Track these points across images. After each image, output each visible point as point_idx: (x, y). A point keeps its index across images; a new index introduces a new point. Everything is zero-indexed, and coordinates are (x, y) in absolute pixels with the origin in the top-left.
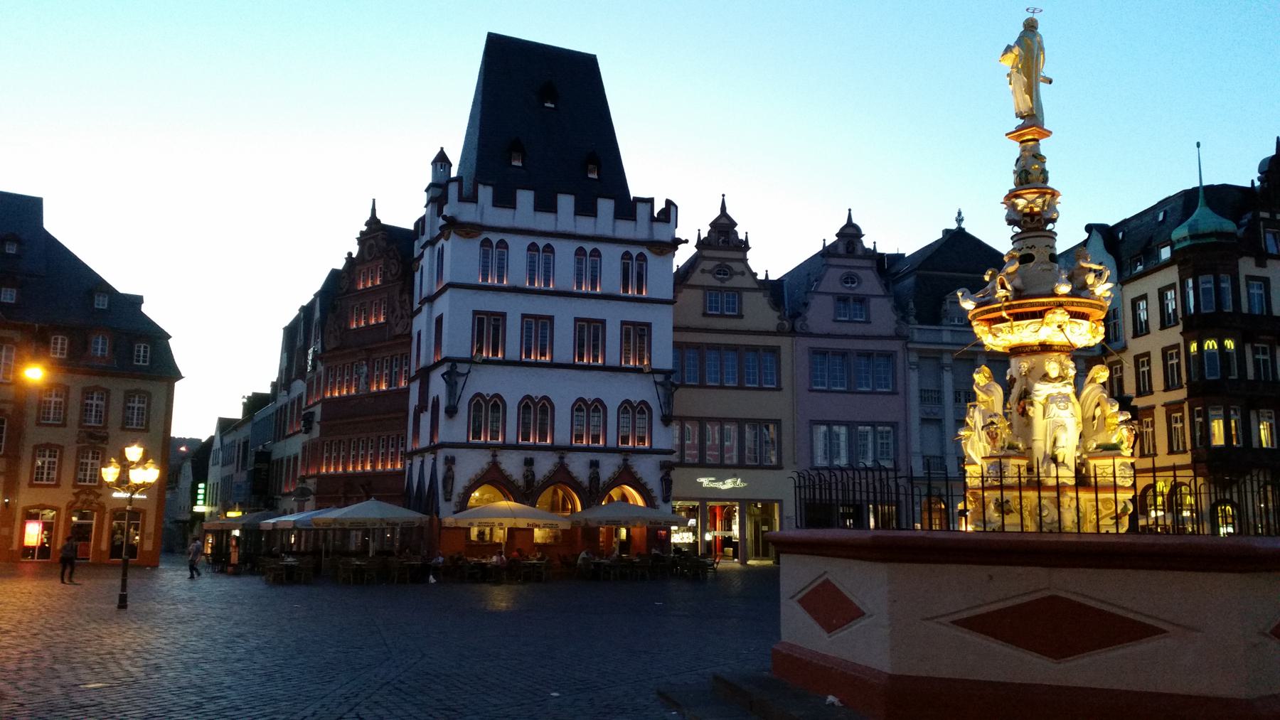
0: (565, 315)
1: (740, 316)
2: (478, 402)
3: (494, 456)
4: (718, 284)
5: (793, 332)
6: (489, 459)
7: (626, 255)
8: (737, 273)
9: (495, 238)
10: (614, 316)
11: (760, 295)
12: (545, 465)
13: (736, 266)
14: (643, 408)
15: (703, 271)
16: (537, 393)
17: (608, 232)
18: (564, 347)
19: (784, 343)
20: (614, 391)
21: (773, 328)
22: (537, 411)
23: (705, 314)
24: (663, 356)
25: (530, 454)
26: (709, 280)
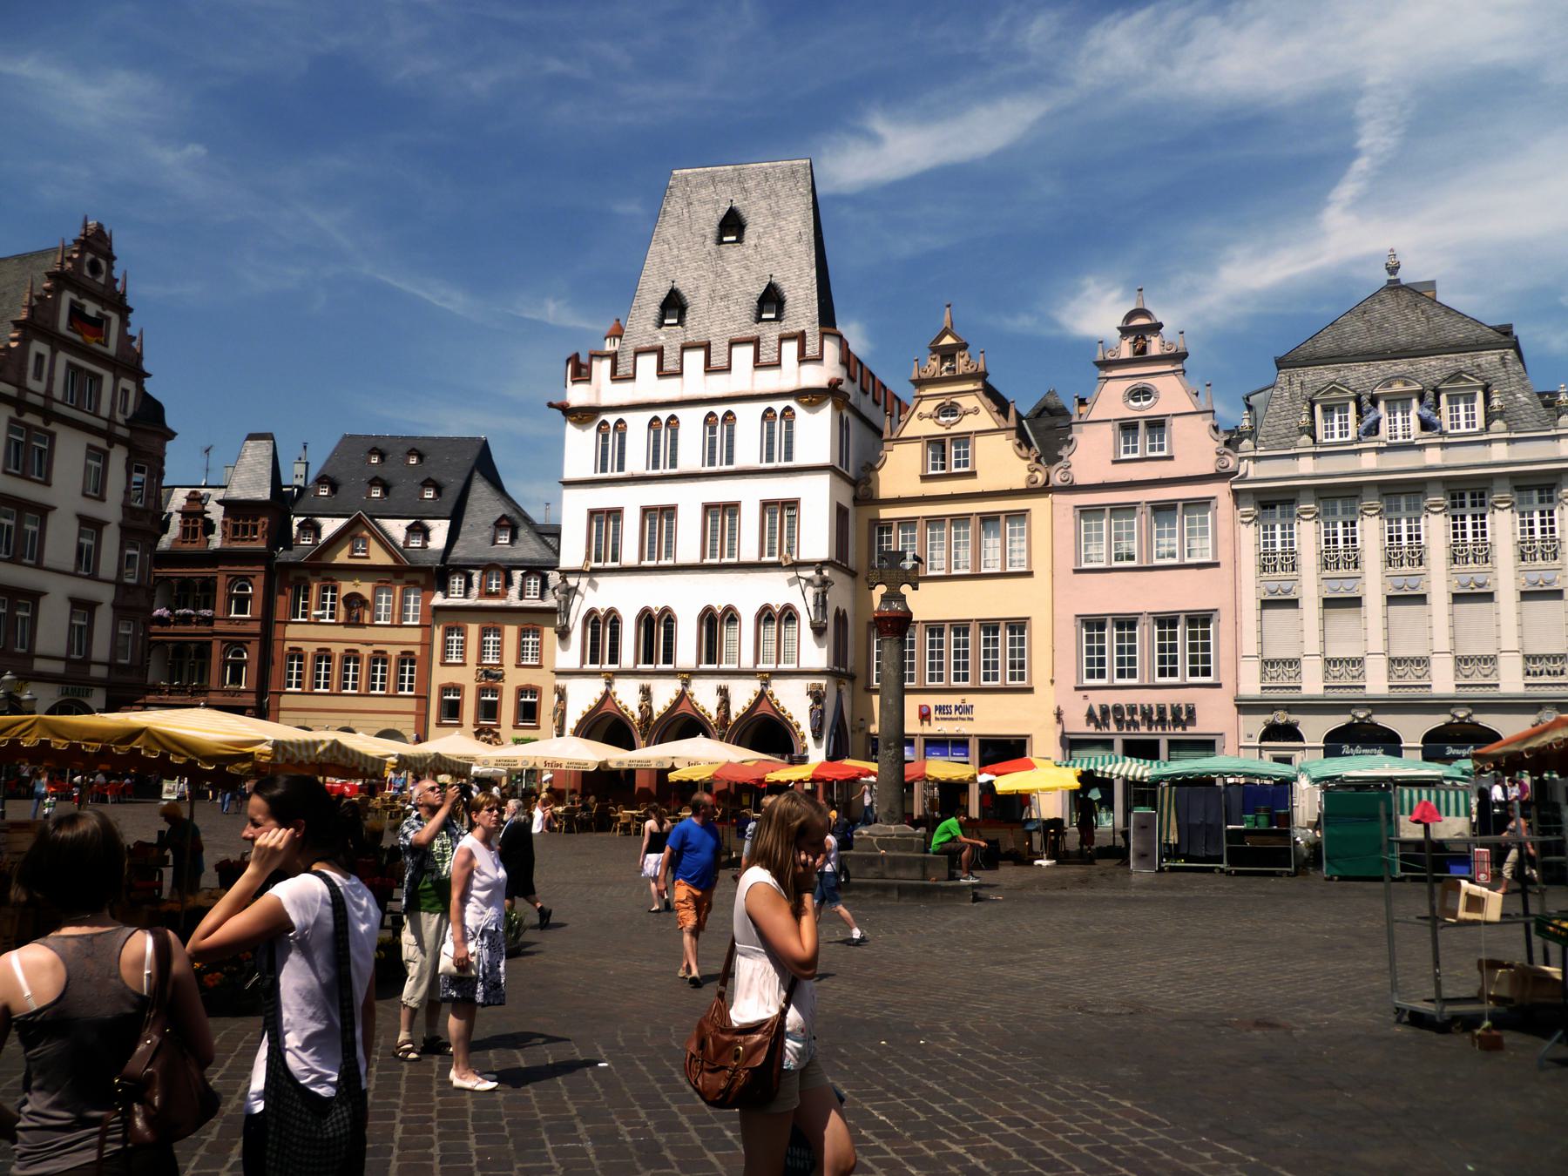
0: (689, 500)
1: (973, 474)
2: (593, 620)
3: (609, 684)
4: (942, 431)
5: (1046, 490)
6: (603, 688)
7: (768, 415)
8: (965, 413)
9: (611, 419)
10: (750, 494)
11: (1002, 437)
12: (664, 694)
13: (967, 402)
14: (789, 615)
15: (921, 417)
16: (656, 605)
17: (746, 389)
18: (688, 543)
19: (1038, 507)
20: (748, 594)
21: (1023, 485)
22: (656, 628)
23: (925, 478)
24: (815, 540)
25: (646, 682)
26: (931, 428)
